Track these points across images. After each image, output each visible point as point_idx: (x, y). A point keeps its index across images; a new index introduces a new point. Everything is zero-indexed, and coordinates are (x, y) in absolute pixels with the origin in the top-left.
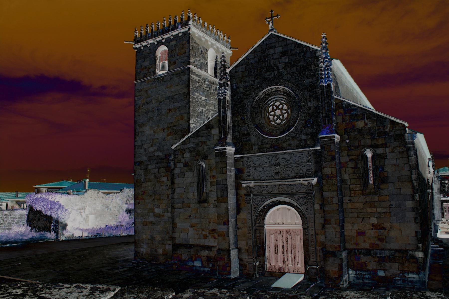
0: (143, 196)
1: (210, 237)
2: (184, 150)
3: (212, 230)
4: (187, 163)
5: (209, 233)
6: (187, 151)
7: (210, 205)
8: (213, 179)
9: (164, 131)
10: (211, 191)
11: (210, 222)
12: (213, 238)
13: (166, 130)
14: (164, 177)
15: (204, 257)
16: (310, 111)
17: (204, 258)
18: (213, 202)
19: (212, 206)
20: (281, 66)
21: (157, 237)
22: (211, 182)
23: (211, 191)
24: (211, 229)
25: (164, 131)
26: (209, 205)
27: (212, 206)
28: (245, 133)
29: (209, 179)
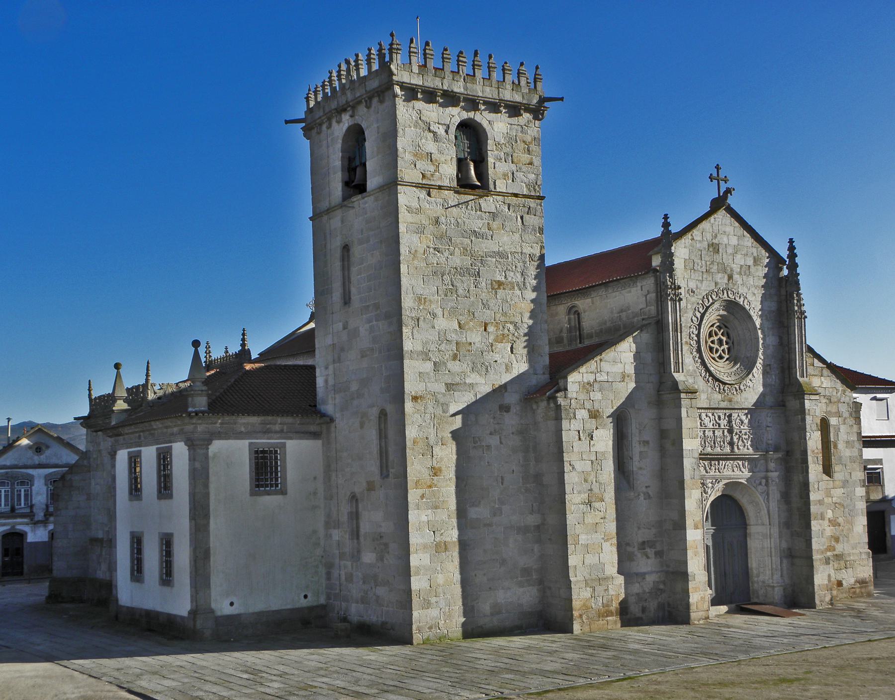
0: (435, 478)
1: (639, 555)
2: (588, 383)
3: (644, 543)
4: (598, 411)
5: (639, 549)
6: (596, 386)
7: (639, 495)
8: (645, 445)
9: (485, 330)
10: (641, 468)
11: (639, 528)
12: (645, 557)
13: (491, 329)
14: (491, 434)
15: (633, 595)
16: (769, 351)
17: (633, 597)
18: (644, 489)
19: (642, 497)
20: (736, 268)
21: (476, 575)
22: (641, 452)
23: (641, 468)
24: (640, 540)
25: (485, 330)
26: (636, 495)
27: (642, 497)
28: (690, 370)
29: (637, 445)
